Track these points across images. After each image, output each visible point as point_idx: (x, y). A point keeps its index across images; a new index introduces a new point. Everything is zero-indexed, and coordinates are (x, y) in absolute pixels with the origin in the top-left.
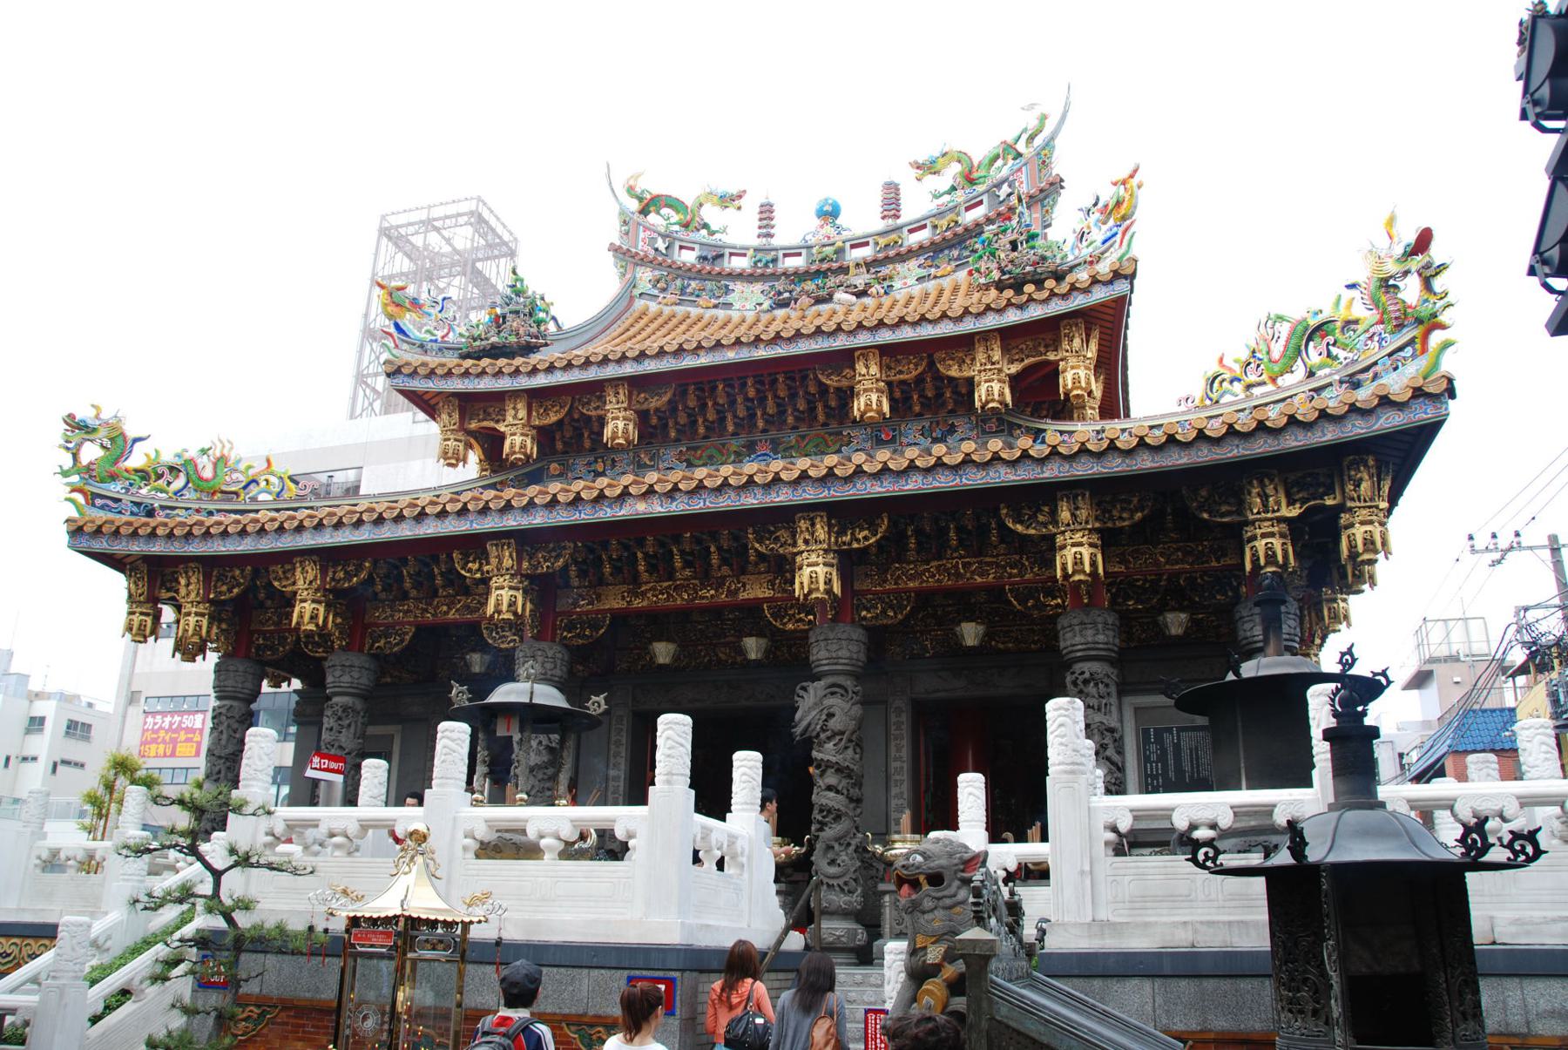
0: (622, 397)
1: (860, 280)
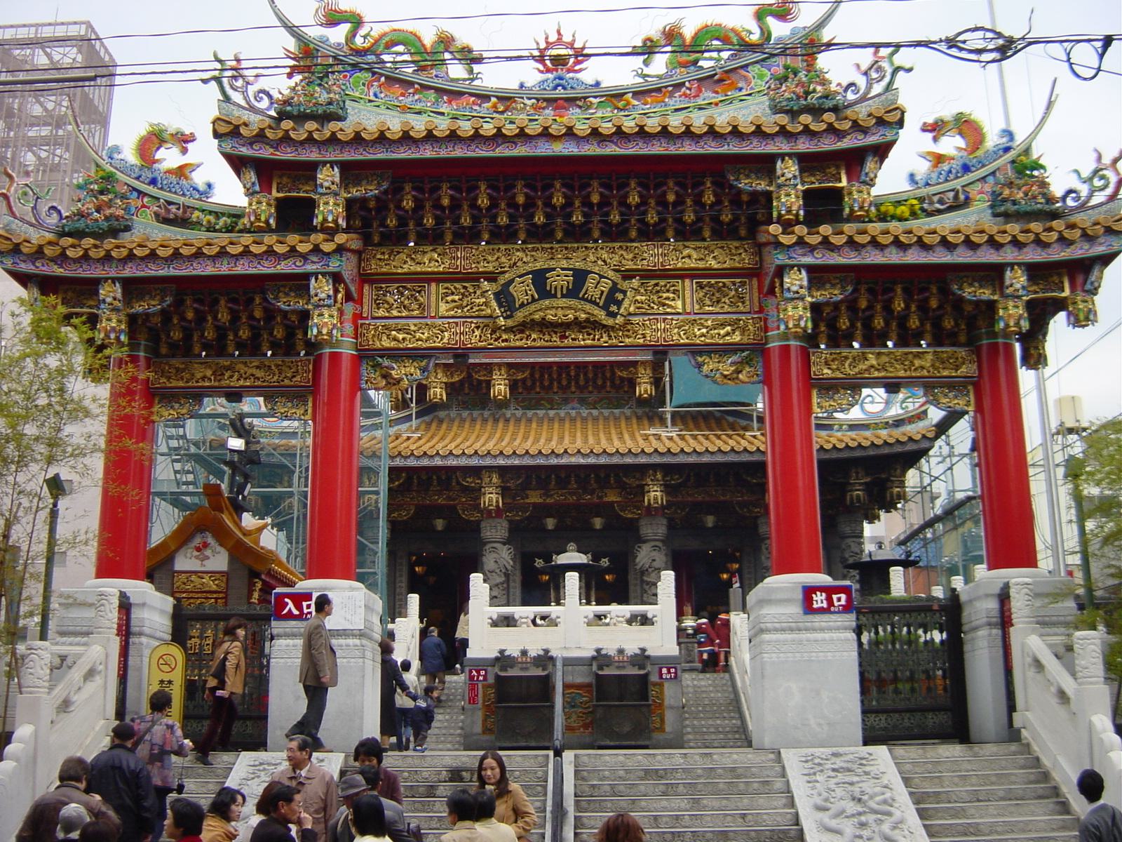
0: (503, 372)
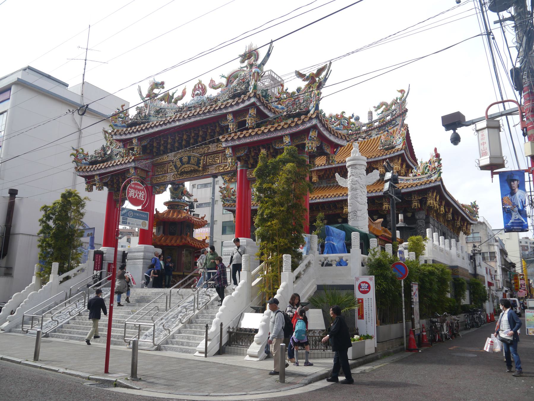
1: (364, 136)
